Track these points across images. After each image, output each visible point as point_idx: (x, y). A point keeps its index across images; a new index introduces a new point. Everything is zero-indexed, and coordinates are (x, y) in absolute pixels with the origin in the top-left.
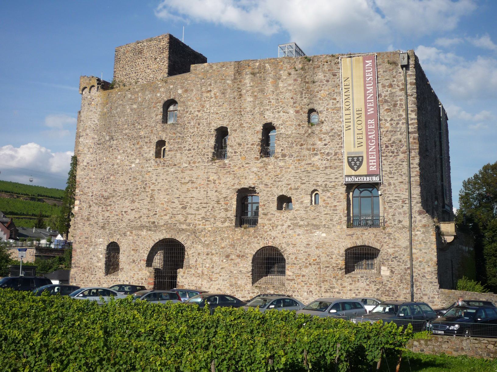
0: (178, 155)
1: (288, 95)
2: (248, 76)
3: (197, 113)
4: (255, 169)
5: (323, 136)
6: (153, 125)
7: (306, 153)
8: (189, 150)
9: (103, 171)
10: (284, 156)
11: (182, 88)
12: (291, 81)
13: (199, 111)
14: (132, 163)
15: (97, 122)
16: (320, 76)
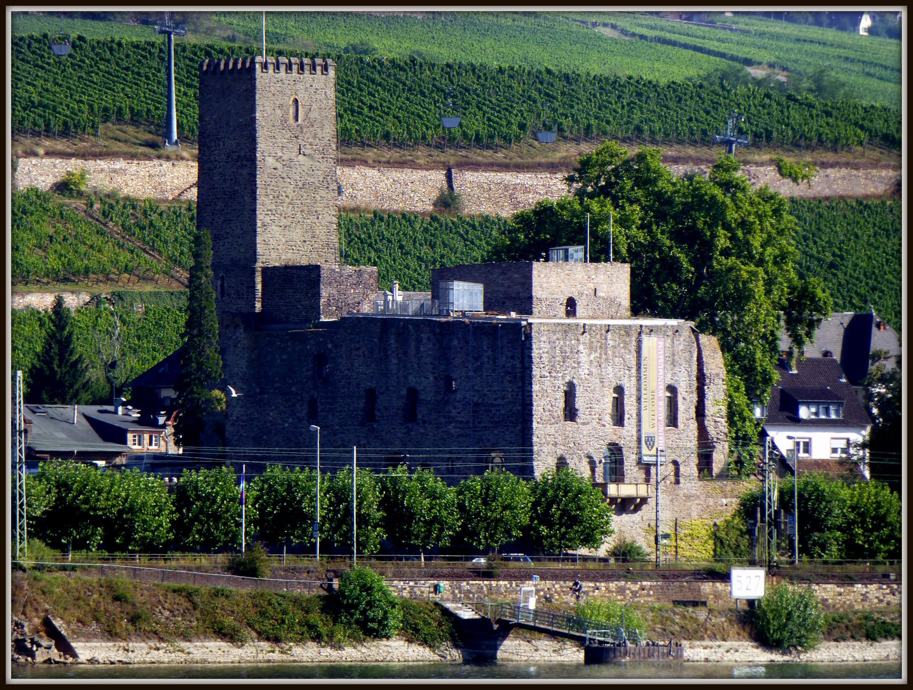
0: (330, 416)
1: (428, 360)
2: (392, 337)
3: (347, 372)
4: (400, 435)
5: (456, 404)
6: (304, 381)
7: (443, 420)
8: (340, 411)
9: (255, 429)
10: (424, 422)
11: (332, 342)
12: (430, 346)
13: (348, 370)
14: (285, 422)
15: (244, 369)
16: (455, 342)
